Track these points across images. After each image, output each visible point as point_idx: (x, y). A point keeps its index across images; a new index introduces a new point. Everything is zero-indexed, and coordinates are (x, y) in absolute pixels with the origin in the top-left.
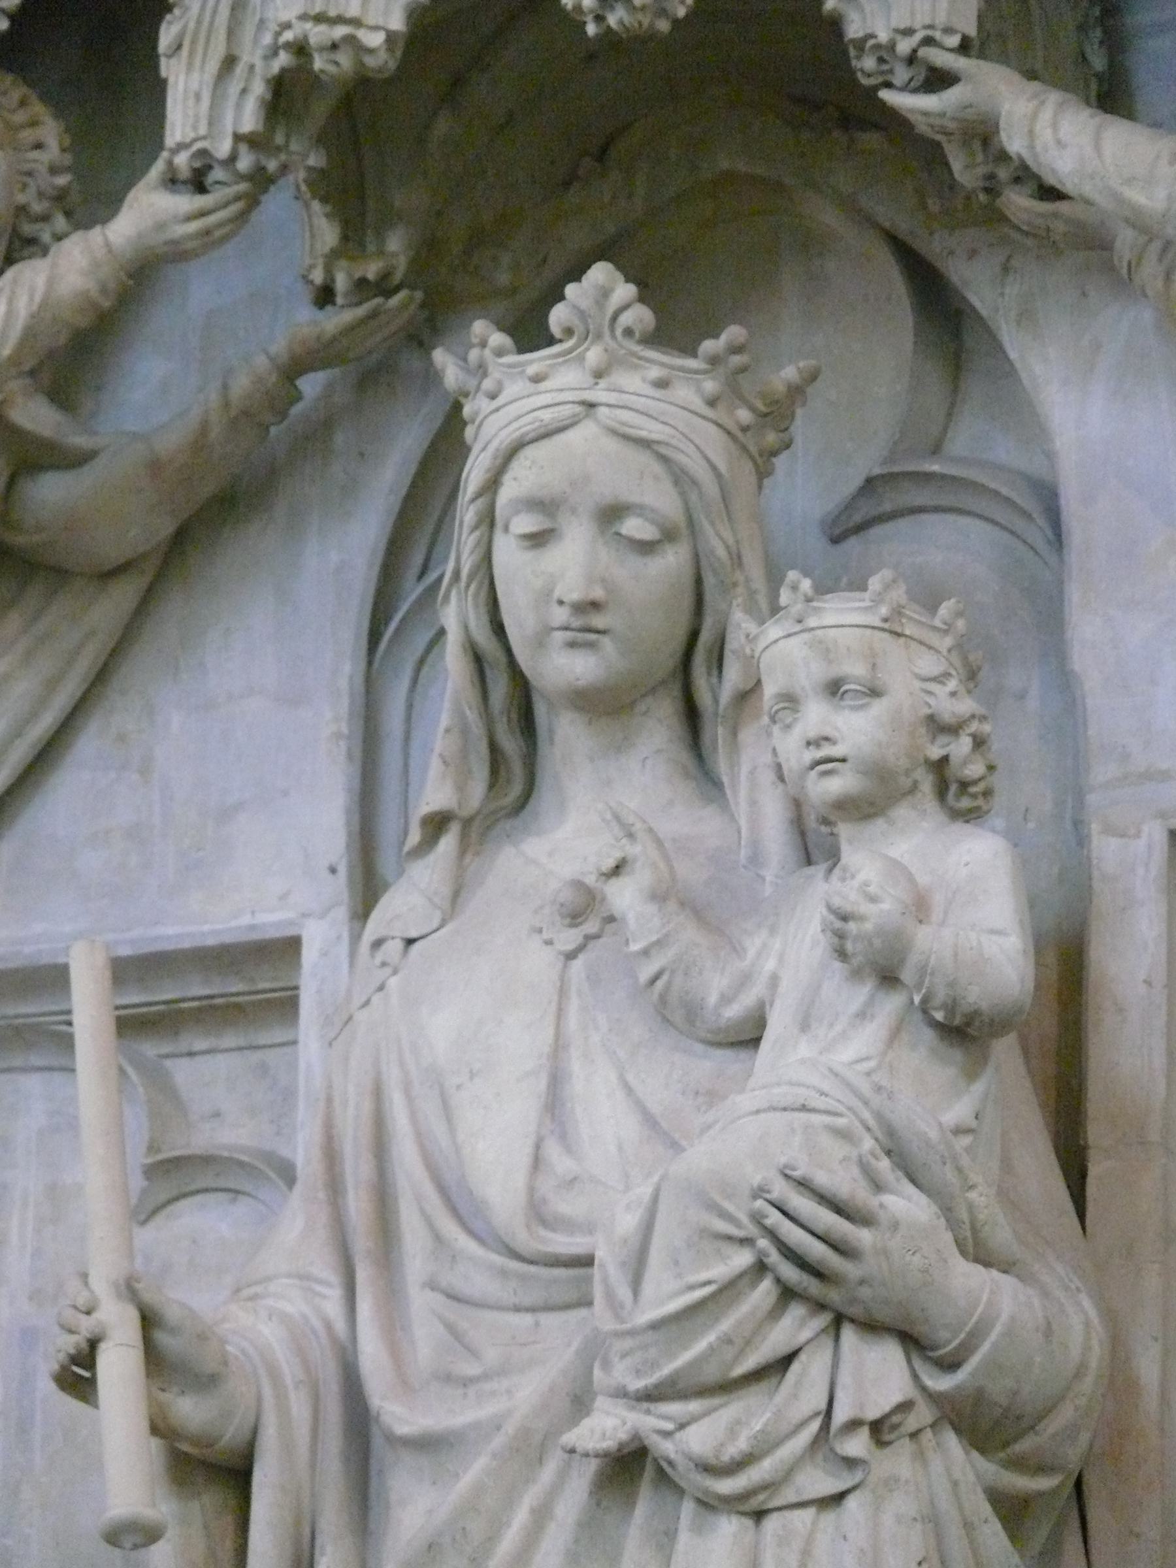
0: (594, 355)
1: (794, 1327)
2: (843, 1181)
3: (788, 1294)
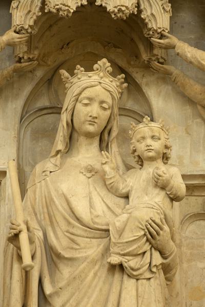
0: (102, 74)
1: (147, 247)
2: (158, 221)
3: (148, 240)
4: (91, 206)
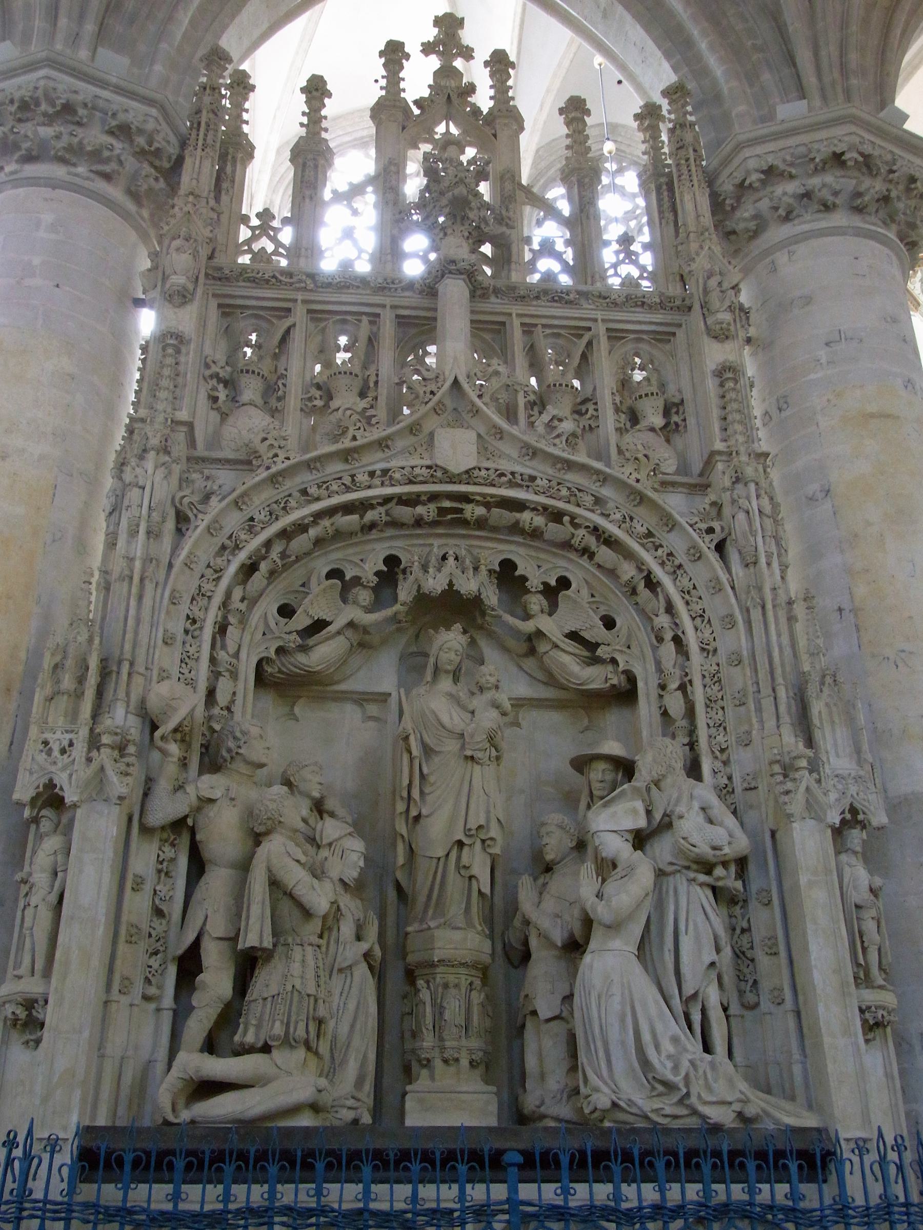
1: (488, 745)
4: (451, 718)
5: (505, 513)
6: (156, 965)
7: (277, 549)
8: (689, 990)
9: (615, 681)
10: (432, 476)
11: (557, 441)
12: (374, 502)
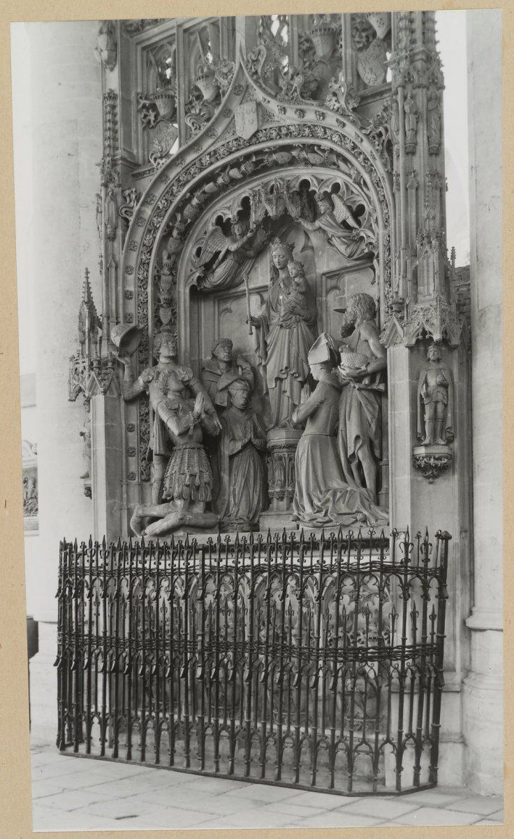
5: (283, 154)
6: (144, 465)
7: (179, 217)
8: (350, 452)
9: (366, 251)
10: (239, 145)
11: (295, 94)
12: (217, 172)
